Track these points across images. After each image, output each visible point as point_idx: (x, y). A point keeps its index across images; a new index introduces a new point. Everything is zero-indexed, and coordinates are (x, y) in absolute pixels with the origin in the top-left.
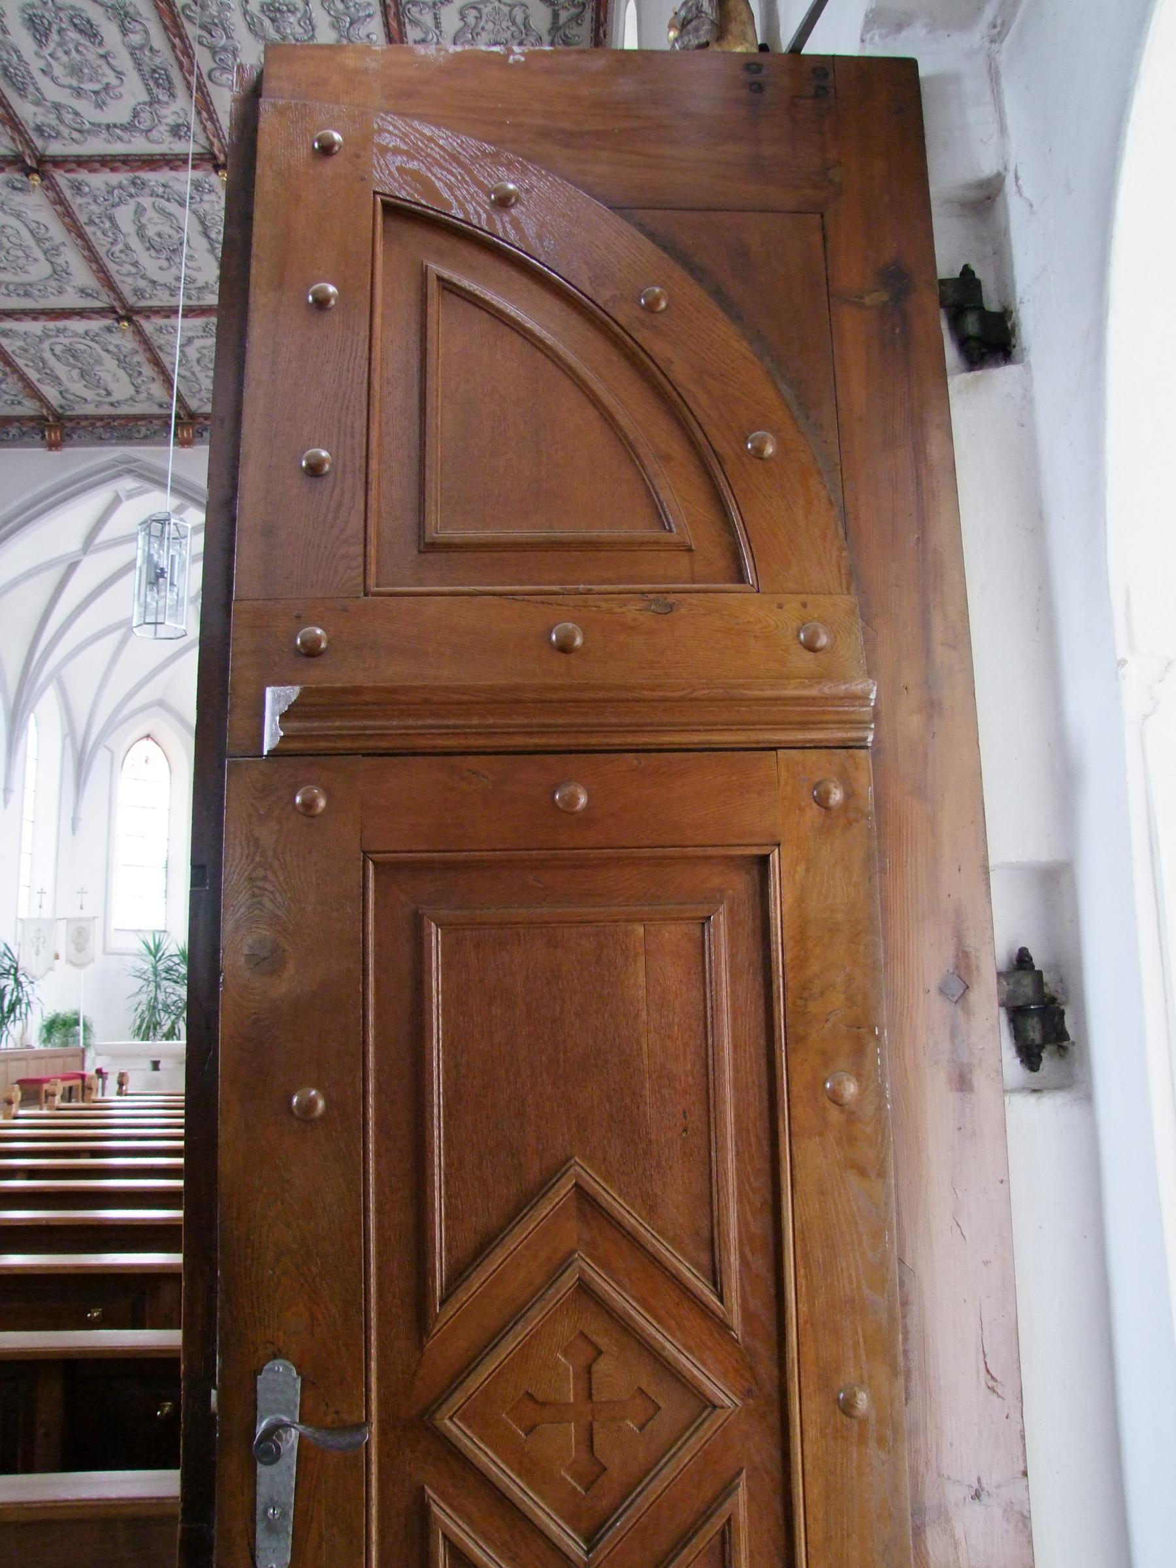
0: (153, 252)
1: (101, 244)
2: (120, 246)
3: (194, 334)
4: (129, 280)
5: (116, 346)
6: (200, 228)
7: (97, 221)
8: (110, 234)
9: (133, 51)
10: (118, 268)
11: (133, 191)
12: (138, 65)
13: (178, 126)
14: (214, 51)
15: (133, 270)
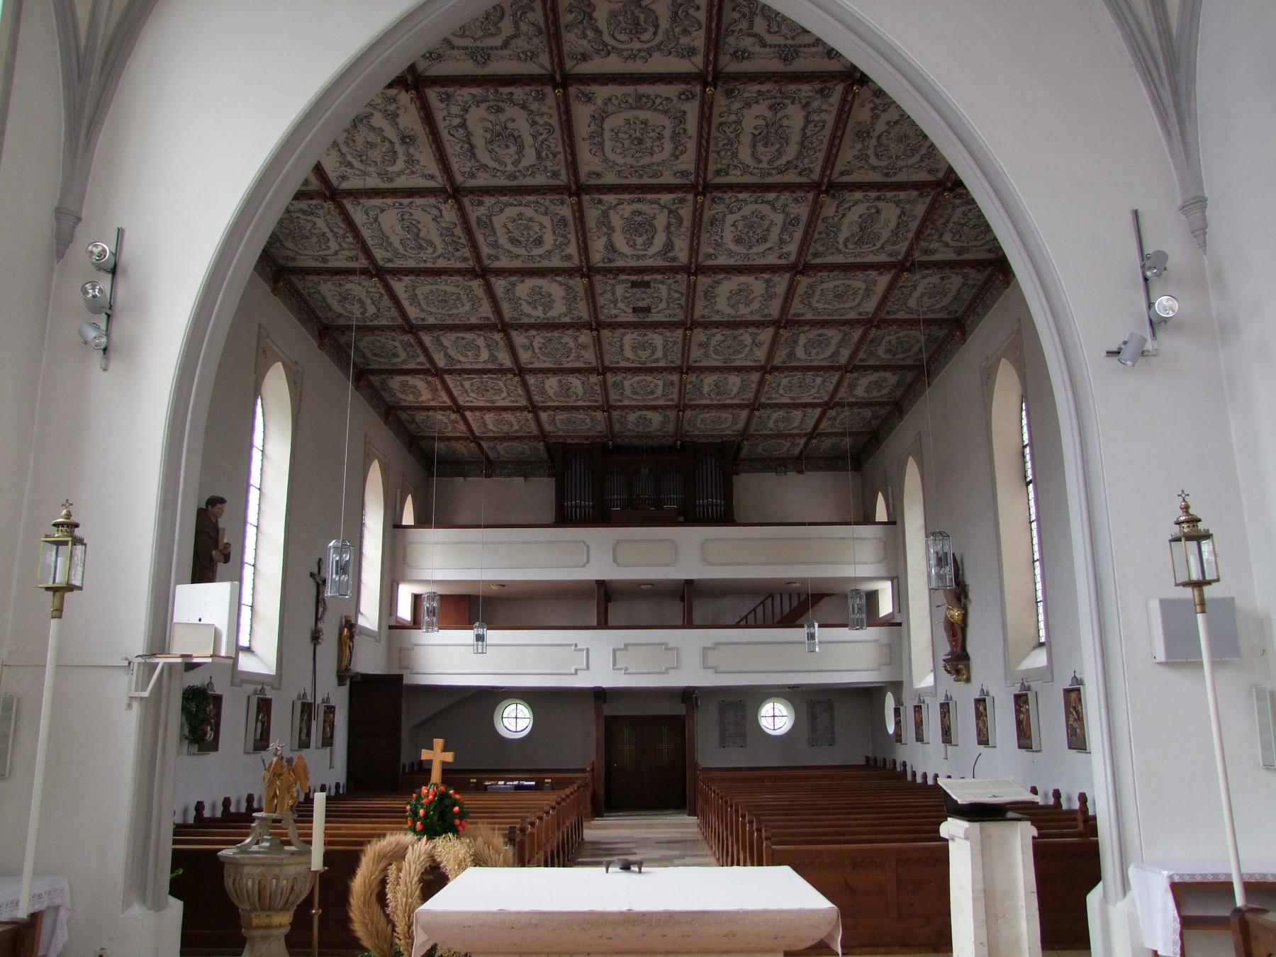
0: (516, 134)
1: (556, 143)
2: (541, 138)
3: (500, 52)
4: (544, 109)
5: (585, 36)
6: (476, 151)
7: (551, 156)
8: (545, 146)
9: (495, 234)
10: (549, 121)
11: (517, 174)
12: (493, 229)
13: (478, 205)
14: (453, 235)
15: (537, 119)
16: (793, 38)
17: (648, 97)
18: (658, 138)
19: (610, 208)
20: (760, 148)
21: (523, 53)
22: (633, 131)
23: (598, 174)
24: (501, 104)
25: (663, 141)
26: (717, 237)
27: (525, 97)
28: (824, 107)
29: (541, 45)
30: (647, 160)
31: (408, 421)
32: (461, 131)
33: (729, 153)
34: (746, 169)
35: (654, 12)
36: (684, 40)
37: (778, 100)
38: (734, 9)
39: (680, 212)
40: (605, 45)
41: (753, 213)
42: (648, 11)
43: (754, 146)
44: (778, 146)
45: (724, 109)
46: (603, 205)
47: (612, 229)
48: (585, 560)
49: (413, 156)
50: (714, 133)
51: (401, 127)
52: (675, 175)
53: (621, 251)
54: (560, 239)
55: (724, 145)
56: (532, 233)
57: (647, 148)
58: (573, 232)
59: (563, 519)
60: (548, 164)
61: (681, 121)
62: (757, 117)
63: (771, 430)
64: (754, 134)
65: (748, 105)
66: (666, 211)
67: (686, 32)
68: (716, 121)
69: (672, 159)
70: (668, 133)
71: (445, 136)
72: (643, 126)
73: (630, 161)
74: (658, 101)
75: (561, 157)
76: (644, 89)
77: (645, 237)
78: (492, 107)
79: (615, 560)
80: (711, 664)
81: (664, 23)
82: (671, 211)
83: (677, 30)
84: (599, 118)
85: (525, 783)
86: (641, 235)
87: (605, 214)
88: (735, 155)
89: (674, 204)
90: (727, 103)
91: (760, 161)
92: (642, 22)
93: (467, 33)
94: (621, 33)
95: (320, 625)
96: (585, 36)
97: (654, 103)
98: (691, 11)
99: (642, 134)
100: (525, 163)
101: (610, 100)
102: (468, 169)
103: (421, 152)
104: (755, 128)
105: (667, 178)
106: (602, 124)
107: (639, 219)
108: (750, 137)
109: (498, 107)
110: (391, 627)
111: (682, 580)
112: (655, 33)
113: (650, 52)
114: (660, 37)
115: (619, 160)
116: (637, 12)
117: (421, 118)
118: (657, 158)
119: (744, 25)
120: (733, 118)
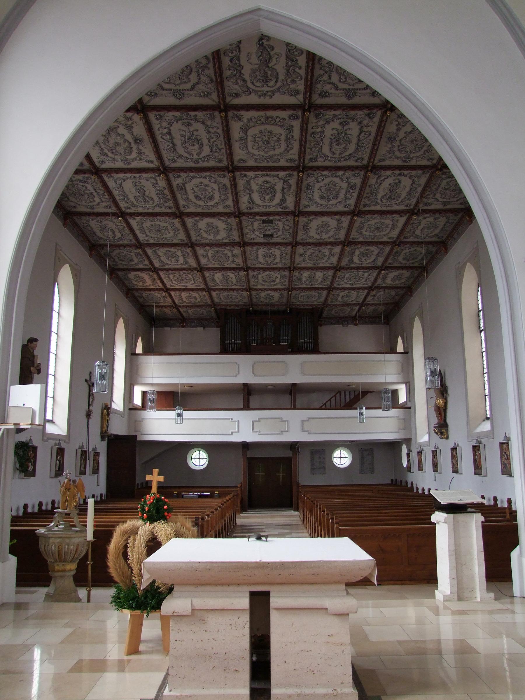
0: (199, 138)
1: (221, 143)
2: (212, 140)
5: (237, 83)
6: (176, 147)
8: (214, 145)
10: (217, 131)
12: (186, 191)
13: (178, 177)
14: (163, 194)
15: (210, 130)
16: (353, 85)
17: (272, 117)
18: (278, 141)
19: (251, 179)
20: (335, 146)
21: (202, 92)
22: (264, 137)
23: (244, 161)
24: (190, 121)
25: (280, 142)
26: (310, 196)
27: (204, 117)
28: (370, 124)
29: (213, 88)
30: (271, 153)
31: (139, 297)
32: (168, 136)
33: (317, 149)
34: (326, 158)
35: (276, 70)
36: (292, 86)
37: (345, 120)
38: (320, 69)
39: (290, 181)
40: (249, 88)
41: (330, 182)
42: (273, 69)
43: (331, 146)
44: (344, 145)
45: (314, 125)
46: (247, 177)
47: (252, 191)
48: (237, 373)
49: (141, 150)
50: (309, 138)
51: (135, 134)
52: (287, 161)
53: (257, 203)
54: (223, 197)
55: (314, 145)
56: (207, 193)
57: (271, 146)
58: (230, 192)
59: (225, 350)
60: (216, 154)
61: (290, 131)
62: (333, 129)
63: (340, 302)
64: (331, 138)
65: (328, 122)
66: (282, 181)
67: (293, 81)
68: (310, 131)
69: (286, 152)
70: (283, 138)
71: (159, 139)
72: (269, 134)
73: (262, 153)
74: (278, 120)
75: (224, 151)
76: (270, 113)
77: (270, 195)
78: (185, 123)
79: (253, 373)
80: (306, 429)
81: (281, 77)
82: (284, 181)
83: (289, 80)
84: (245, 129)
85: (204, 494)
86: (268, 194)
87: (248, 182)
88: (320, 150)
89: (286, 177)
90: (316, 121)
91: (334, 154)
92: (269, 76)
93: (171, 81)
94: (257, 81)
95: (91, 408)
96: (237, 83)
97: (276, 121)
98: (297, 70)
99: (269, 138)
100: (203, 154)
101: (251, 119)
102: (172, 158)
103: (146, 148)
104: (332, 135)
105: (283, 163)
106: (246, 133)
107: (267, 185)
108: (329, 140)
109: (189, 123)
110: (130, 409)
111: (290, 383)
112: (276, 82)
113: (273, 92)
114: (279, 84)
115: (256, 153)
116: (266, 70)
117: (146, 129)
118: (277, 152)
119: (326, 77)
120: (319, 129)
